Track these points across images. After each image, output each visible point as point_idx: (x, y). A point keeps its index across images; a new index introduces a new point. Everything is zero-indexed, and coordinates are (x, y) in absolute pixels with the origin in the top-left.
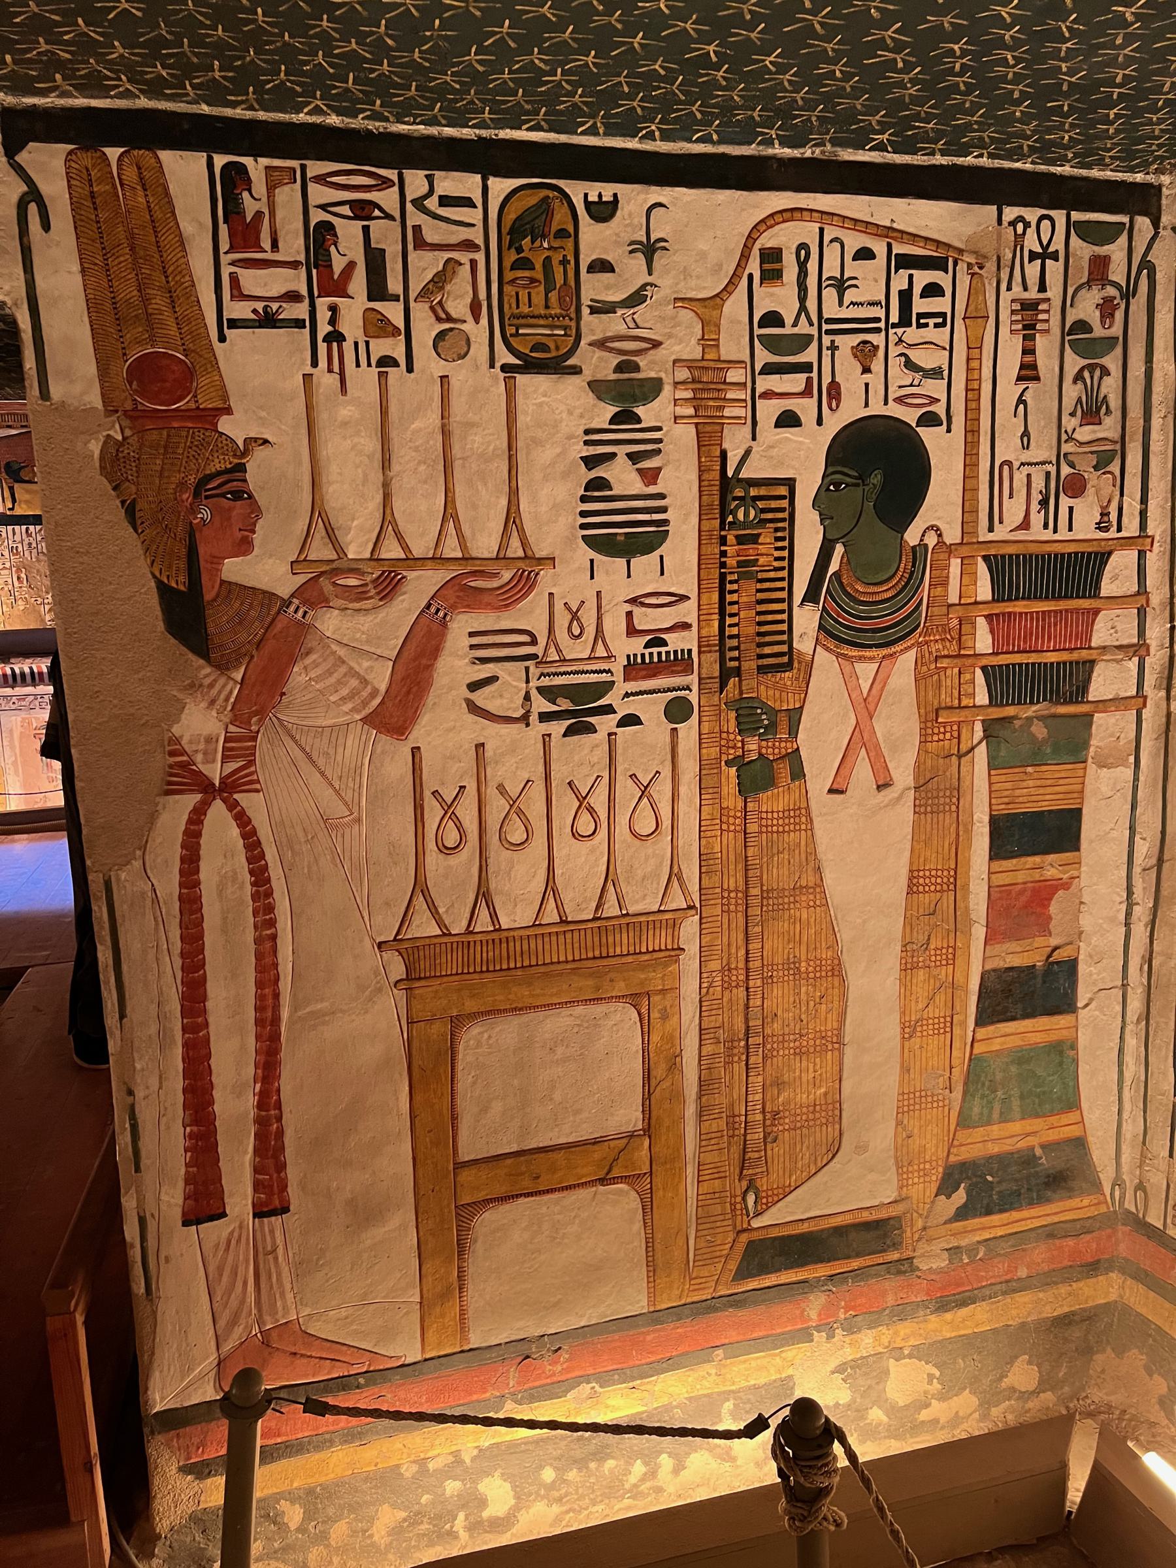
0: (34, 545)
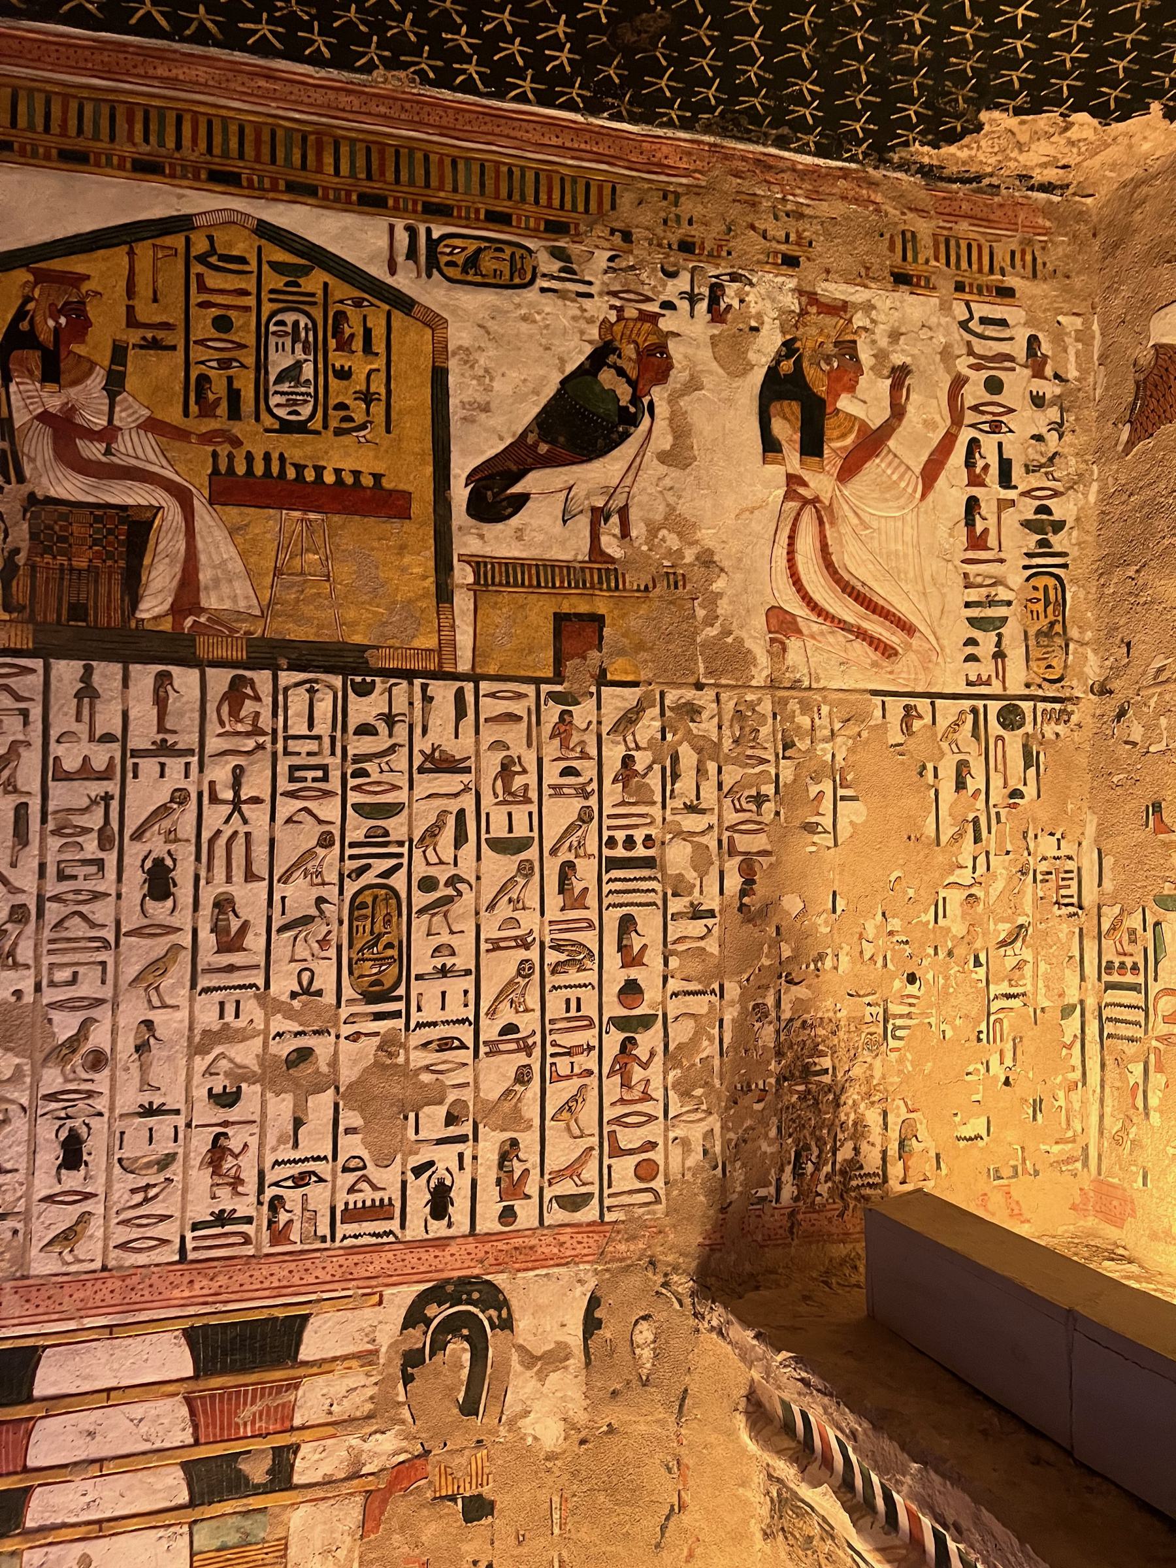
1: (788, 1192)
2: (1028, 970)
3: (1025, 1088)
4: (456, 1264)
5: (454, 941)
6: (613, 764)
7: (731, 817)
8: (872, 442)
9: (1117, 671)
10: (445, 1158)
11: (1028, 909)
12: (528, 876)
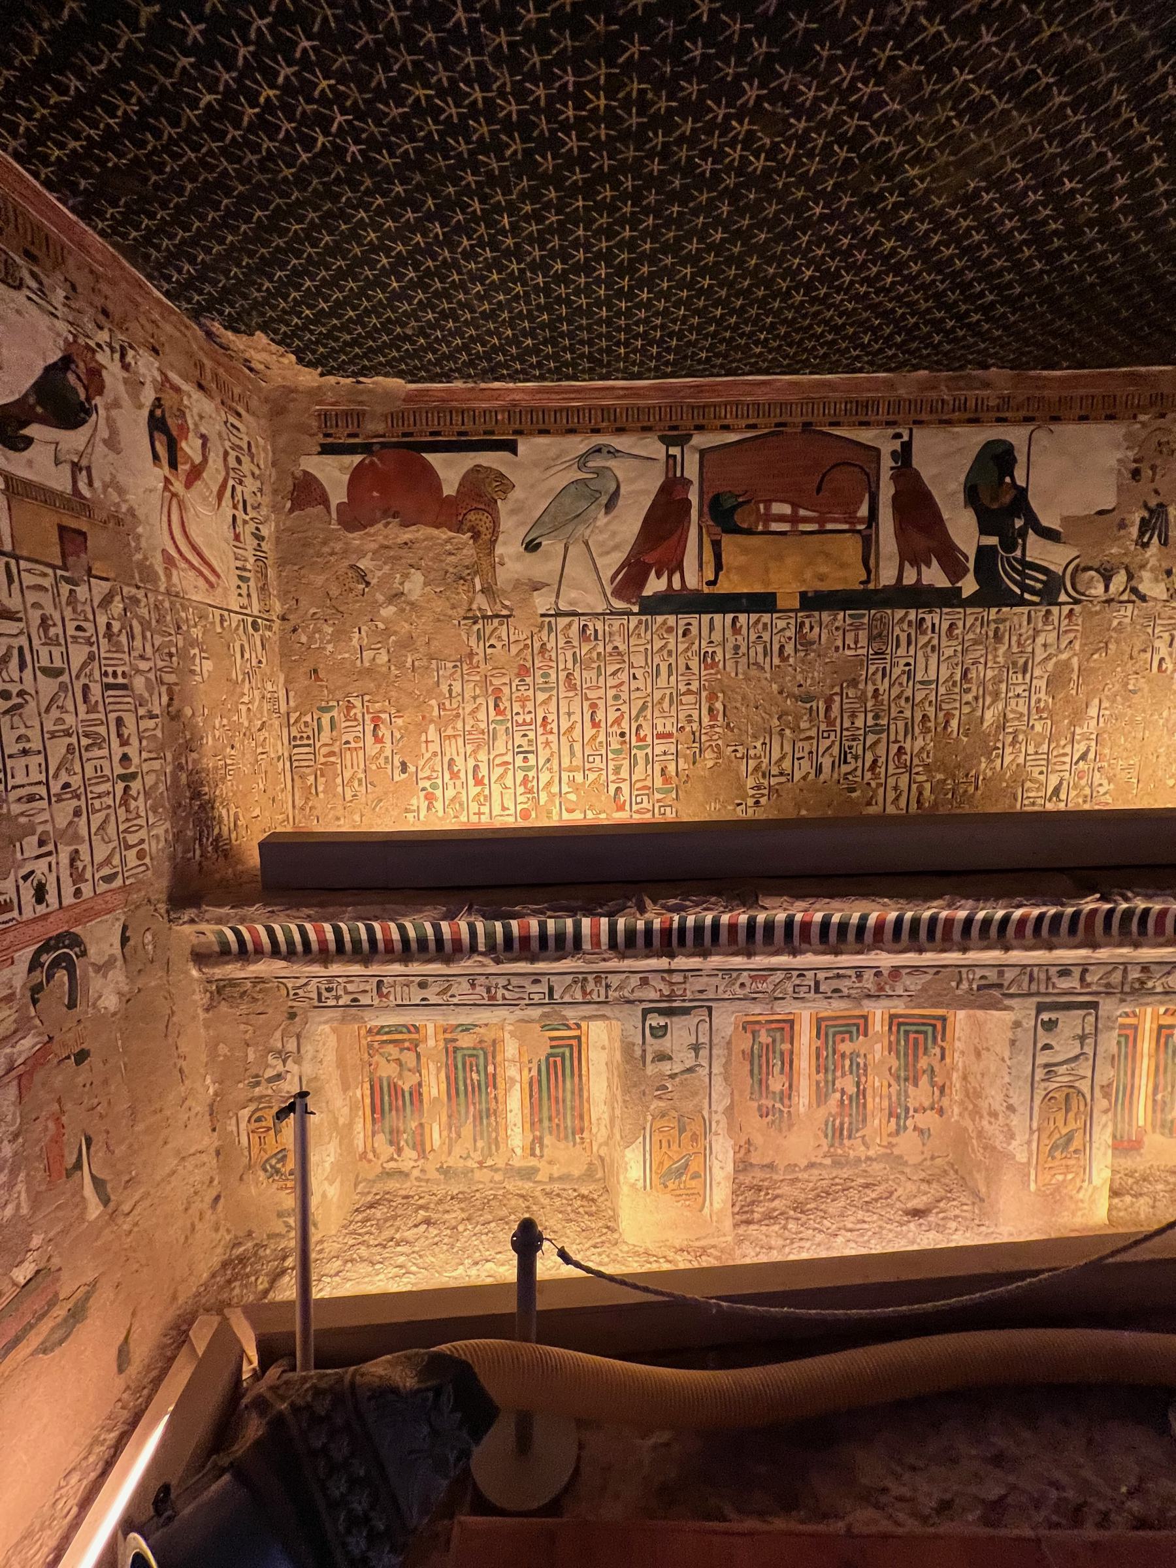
0: (743, 650)
1: (198, 853)
3: (270, 793)
4: (54, 928)
5: (29, 733)
6: (102, 630)
7: (160, 664)
8: (195, 473)
10: (41, 866)
12: (66, 691)
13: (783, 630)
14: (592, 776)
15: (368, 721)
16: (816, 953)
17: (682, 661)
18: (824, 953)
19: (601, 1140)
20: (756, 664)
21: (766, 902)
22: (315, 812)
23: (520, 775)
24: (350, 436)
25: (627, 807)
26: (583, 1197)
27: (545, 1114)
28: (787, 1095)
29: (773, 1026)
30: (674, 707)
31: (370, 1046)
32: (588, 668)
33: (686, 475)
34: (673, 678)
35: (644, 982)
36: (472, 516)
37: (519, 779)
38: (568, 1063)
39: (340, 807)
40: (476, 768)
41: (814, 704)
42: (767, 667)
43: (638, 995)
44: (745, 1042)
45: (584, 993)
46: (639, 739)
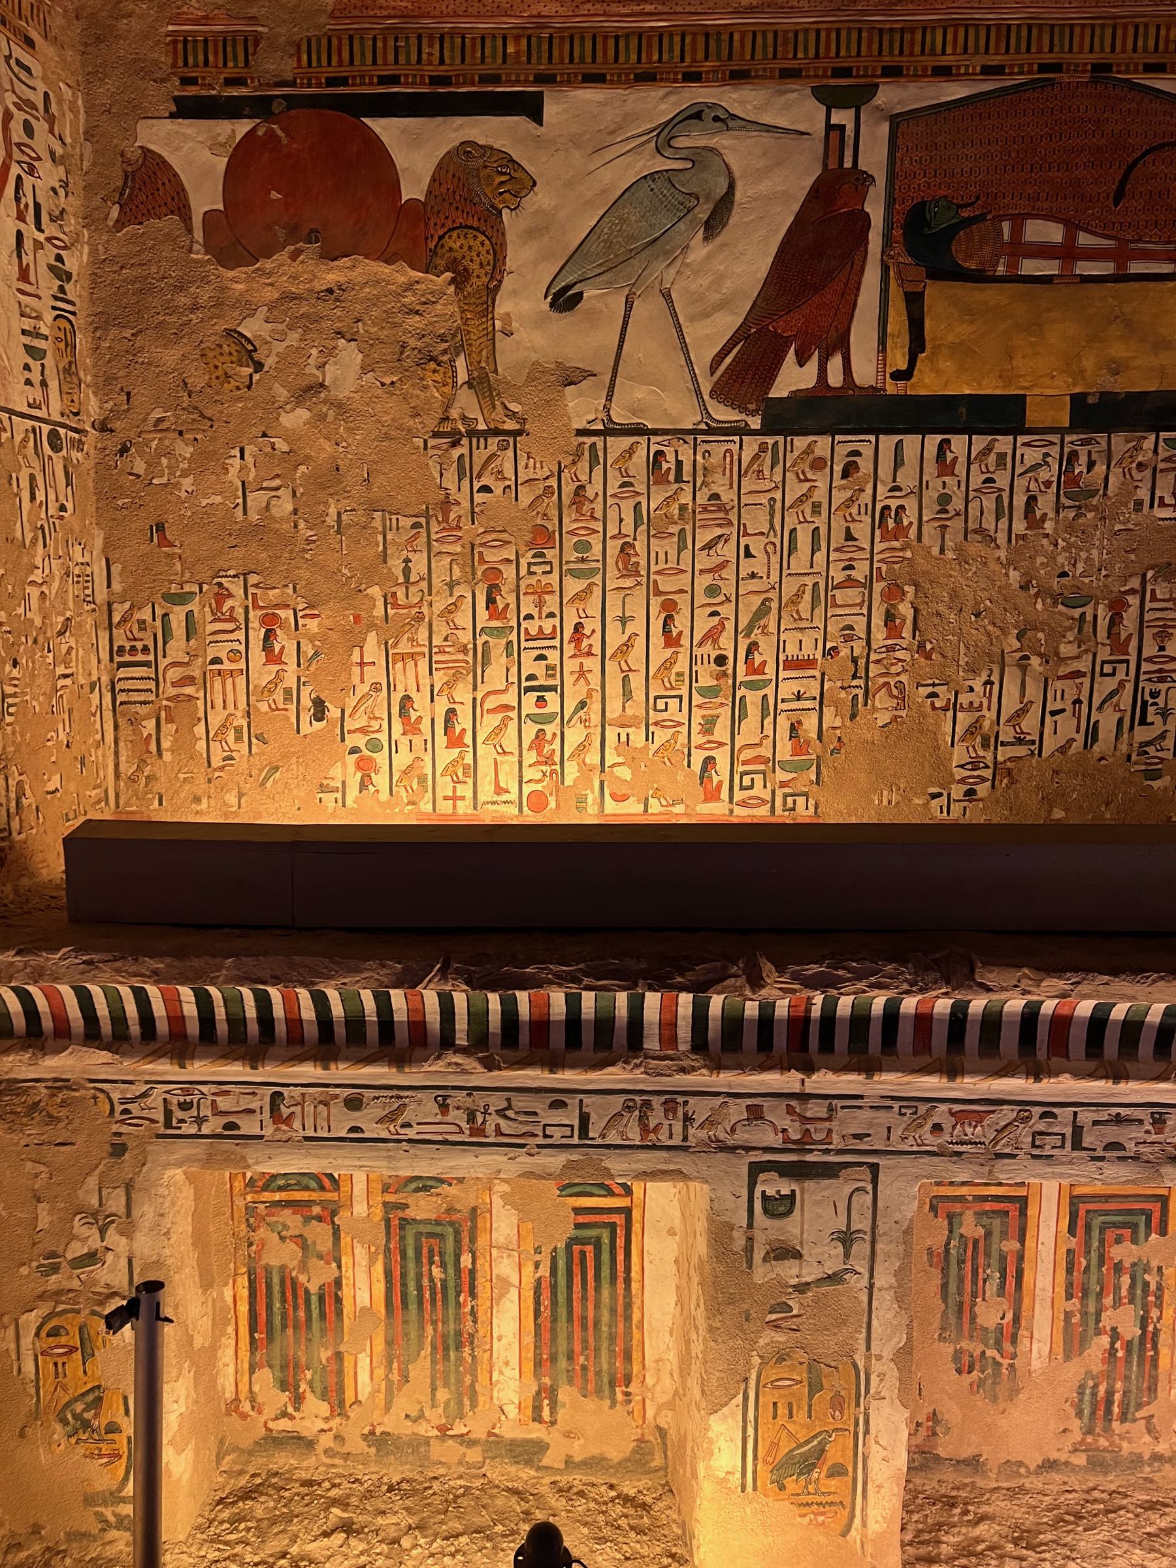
0: (957, 504)
2: (74, 653)
9: (115, 413)
11: (71, 605)
13: (1034, 468)
14: (661, 736)
15: (254, 623)
16: (1078, 1074)
17: (838, 525)
18: (1093, 1076)
19: (663, 1399)
20: (980, 531)
21: (991, 977)
22: (158, 787)
23: (530, 731)
24: (230, 82)
25: (725, 794)
26: (626, 1500)
27: (562, 1346)
28: (1011, 1333)
29: (988, 1206)
30: (819, 611)
31: (250, 1210)
32: (663, 535)
33: (862, 166)
34: (820, 557)
35: (755, 1113)
36: (454, 242)
37: (527, 739)
38: (605, 1256)
39: (202, 780)
40: (451, 714)
41: (1089, 610)
42: (1002, 538)
43: (741, 1137)
44: (935, 1235)
45: (645, 1129)
46: (752, 670)
